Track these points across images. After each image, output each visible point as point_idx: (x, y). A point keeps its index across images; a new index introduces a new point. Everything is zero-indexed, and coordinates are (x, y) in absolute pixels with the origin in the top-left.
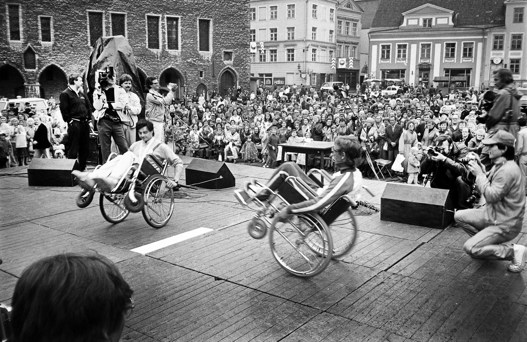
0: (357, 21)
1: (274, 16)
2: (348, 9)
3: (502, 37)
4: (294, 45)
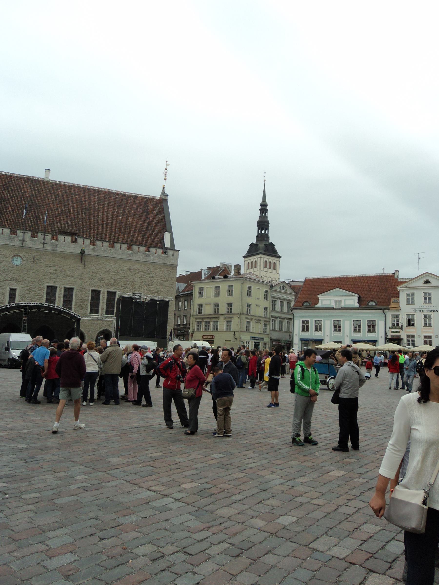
0: (291, 301)
1: (217, 294)
2: (282, 290)
3: (397, 317)
4: (231, 318)
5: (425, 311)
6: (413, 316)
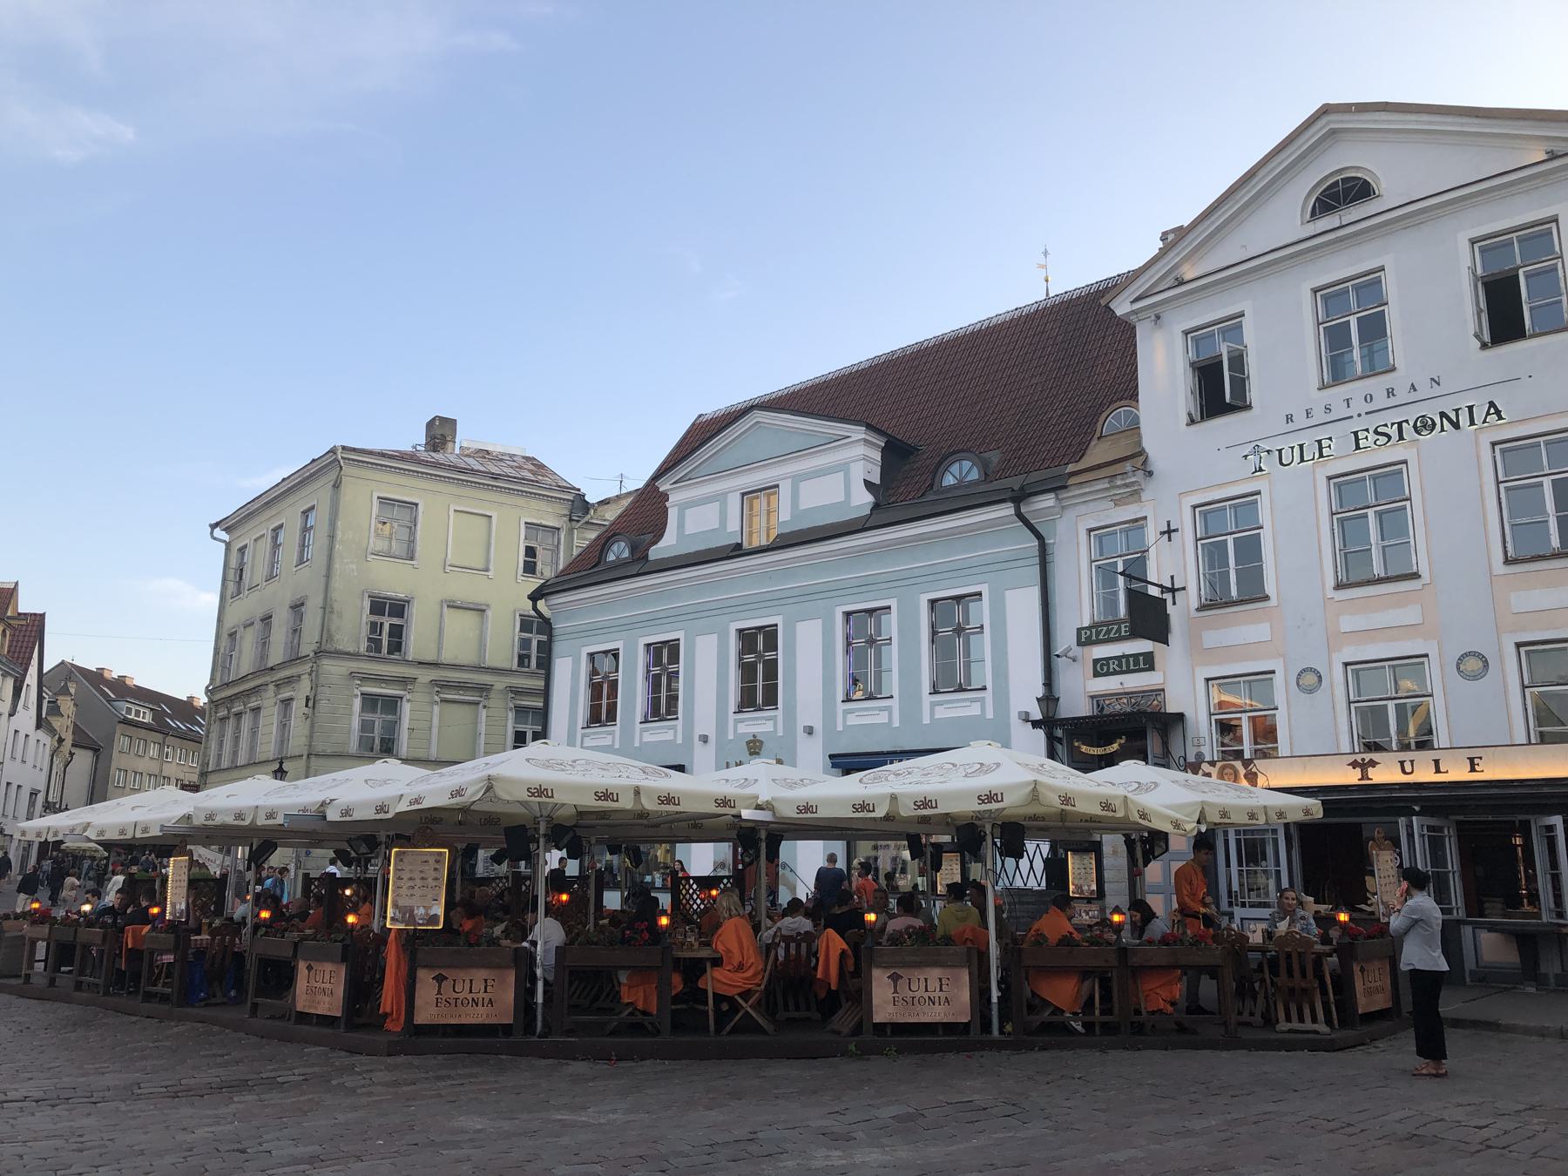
5: (1339, 445)
6: (1247, 503)
